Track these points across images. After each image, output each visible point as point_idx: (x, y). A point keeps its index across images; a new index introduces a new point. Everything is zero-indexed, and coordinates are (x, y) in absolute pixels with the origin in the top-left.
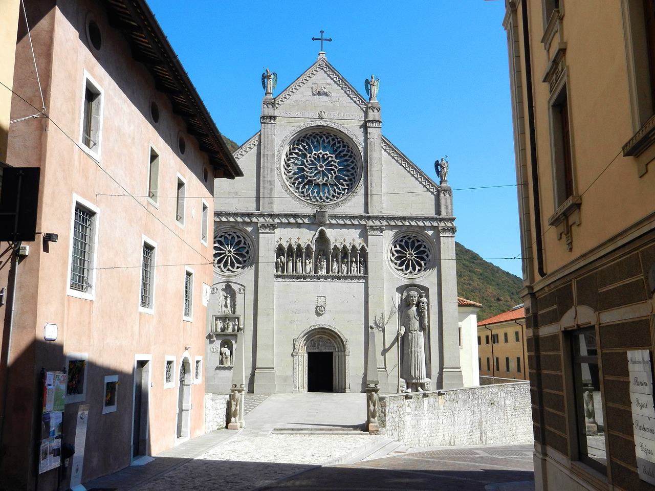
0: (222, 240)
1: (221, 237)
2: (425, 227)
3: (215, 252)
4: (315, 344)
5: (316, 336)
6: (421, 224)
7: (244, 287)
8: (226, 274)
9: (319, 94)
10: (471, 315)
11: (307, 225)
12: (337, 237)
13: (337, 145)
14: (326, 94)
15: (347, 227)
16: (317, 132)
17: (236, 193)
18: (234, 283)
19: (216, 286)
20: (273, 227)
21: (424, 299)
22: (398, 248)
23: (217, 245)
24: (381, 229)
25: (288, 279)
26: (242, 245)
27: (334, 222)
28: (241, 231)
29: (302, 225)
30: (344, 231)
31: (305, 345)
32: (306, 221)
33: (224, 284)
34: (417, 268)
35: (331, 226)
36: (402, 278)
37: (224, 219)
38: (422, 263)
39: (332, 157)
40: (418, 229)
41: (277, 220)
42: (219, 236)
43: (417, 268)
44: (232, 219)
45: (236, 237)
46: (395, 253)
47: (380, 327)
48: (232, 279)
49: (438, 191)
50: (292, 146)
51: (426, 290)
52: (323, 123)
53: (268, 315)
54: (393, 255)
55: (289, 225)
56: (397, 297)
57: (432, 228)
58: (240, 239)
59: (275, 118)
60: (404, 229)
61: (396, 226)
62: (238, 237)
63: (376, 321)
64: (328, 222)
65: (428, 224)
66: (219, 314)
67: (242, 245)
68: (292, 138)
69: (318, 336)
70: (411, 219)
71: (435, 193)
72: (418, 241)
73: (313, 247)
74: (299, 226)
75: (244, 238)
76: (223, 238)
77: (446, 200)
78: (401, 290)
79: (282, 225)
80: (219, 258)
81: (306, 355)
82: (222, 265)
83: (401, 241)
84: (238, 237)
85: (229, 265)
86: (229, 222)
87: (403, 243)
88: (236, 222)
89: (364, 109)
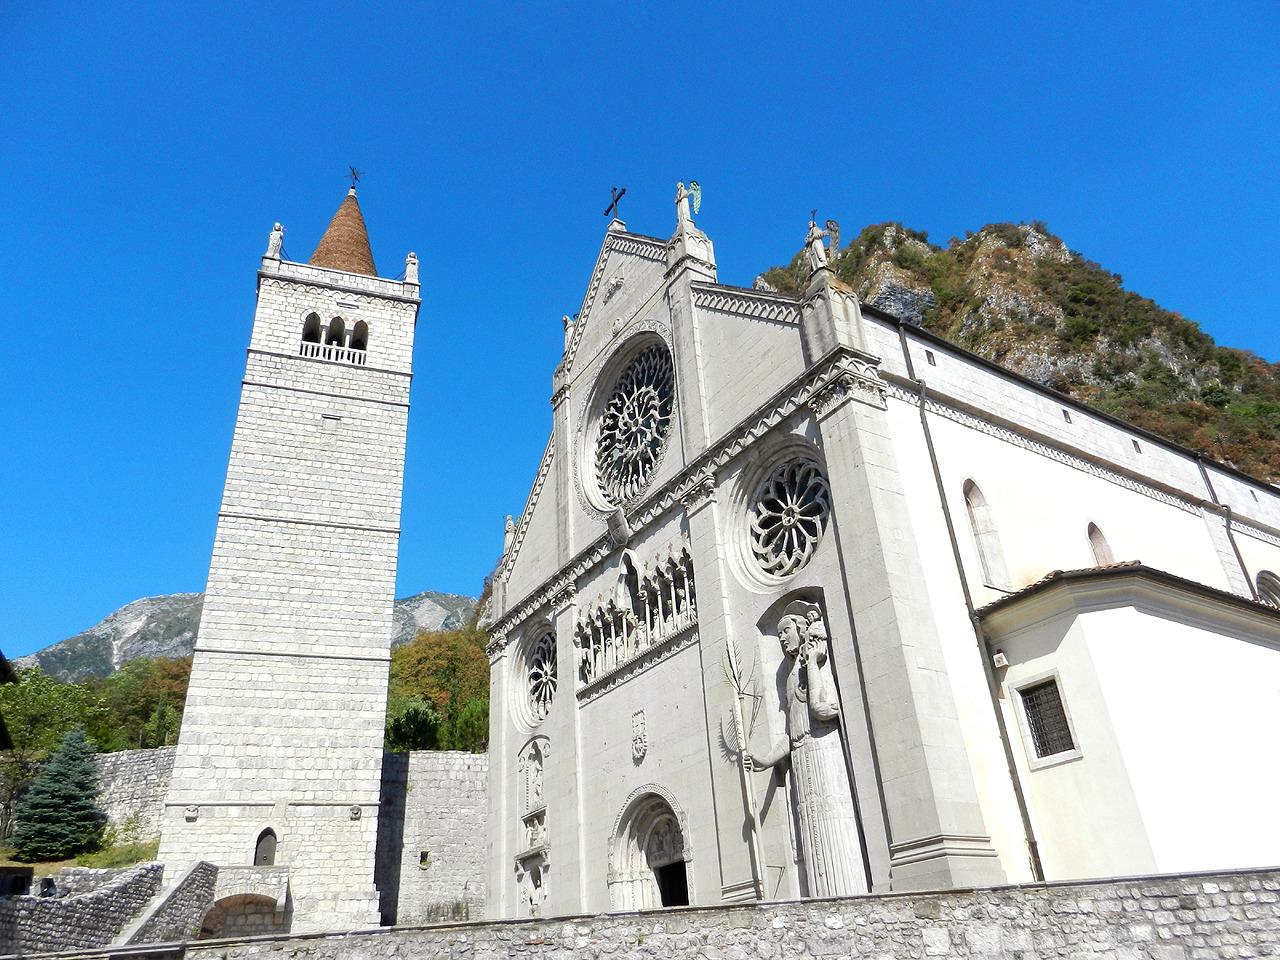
2: (787, 423)
4: (661, 843)
5: (656, 821)
6: (774, 420)
7: (547, 738)
9: (611, 294)
10: (1081, 617)
11: (610, 561)
12: (646, 558)
13: (653, 365)
14: (618, 286)
15: (662, 522)
16: (627, 363)
18: (541, 736)
20: (567, 594)
21: (818, 628)
22: (766, 513)
23: (535, 670)
24: (704, 490)
25: (595, 696)
27: (638, 526)
29: (605, 565)
30: (660, 533)
31: (641, 850)
32: (605, 552)
33: (531, 744)
34: (810, 539)
35: (640, 536)
36: (766, 589)
37: (523, 616)
38: (817, 520)
39: (648, 392)
40: (779, 438)
41: (573, 577)
43: (810, 539)
44: (530, 611)
46: (759, 530)
47: (734, 753)
49: (799, 309)
50: (602, 418)
51: (814, 595)
52: (620, 341)
53: (570, 791)
54: (757, 537)
55: (590, 574)
56: (769, 653)
57: (803, 411)
59: (563, 389)
60: (753, 456)
61: (734, 461)
63: (722, 737)
64: (631, 533)
65: (788, 409)
66: (526, 813)
68: (590, 404)
69: (658, 819)
70: (753, 420)
71: (796, 321)
72: (800, 466)
73: (624, 602)
74: (598, 569)
77: (816, 317)
78: (768, 623)
79: (580, 582)
80: (537, 694)
81: (652, 876)
83: (767, 491)
86: (530, 617)
87: (772, 495)
89: (665, 260)
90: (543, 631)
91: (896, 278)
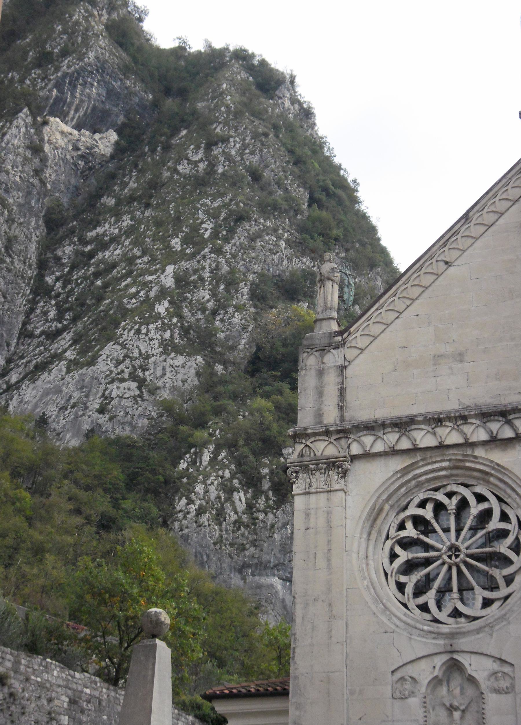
0: (428, 513)
1: (422, 505)
3: (404, 556)
8: (444, 629)
17: (460, 357)
19: (410, 671)
26: (495, 524)
28: (487, 473)
33: (439, 661)
42: (416, 501)
45: (472, 500)
48: (463, 643)
58: (485, 506)
62: (480, 498)
67: (495, 524)
75: (500, 500)
76: (430, 506)
82: (430, 597)
84: (480, 498)
85: (455, 594)
86: (442, 447)
88: (468, 444)
90: (446, 477)
91: (111, 53)
